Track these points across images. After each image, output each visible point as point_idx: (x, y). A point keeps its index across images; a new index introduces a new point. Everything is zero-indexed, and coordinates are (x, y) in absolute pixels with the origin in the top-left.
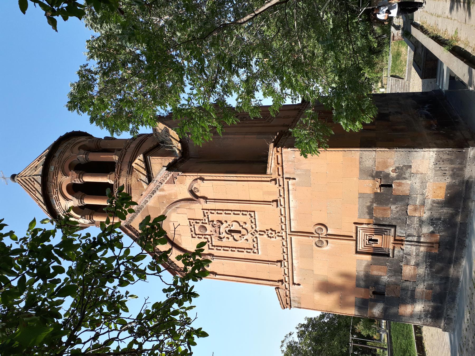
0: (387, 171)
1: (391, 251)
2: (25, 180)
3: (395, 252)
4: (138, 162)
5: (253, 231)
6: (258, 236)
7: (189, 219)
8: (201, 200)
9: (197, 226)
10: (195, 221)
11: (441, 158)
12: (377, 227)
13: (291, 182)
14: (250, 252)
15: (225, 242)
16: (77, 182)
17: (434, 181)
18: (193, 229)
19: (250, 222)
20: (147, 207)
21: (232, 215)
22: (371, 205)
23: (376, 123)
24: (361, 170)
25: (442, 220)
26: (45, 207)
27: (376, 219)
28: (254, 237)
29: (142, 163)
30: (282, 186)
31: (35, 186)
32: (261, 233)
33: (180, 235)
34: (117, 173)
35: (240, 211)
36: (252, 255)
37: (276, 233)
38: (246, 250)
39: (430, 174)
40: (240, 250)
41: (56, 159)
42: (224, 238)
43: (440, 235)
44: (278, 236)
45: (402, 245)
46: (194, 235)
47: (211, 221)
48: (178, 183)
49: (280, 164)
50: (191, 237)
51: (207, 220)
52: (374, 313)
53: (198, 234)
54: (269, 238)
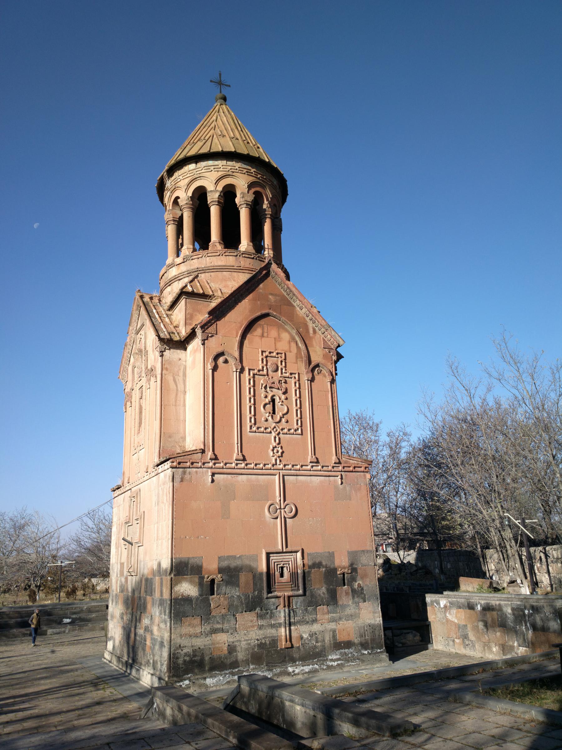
3: (273, 600)
6: (273, 434)
11: (375, 629)
17: (354, 627)
22: (323, 567)
24: (356, 552)
27: (309, 572)
37: (279, 457)
39: (360, 622)
43: (299, 646)
44: (276, 460)
45: (285, 607)
48: (324, 352)
50: (263, 350)
51: (287, 375)
54: (271, 448)
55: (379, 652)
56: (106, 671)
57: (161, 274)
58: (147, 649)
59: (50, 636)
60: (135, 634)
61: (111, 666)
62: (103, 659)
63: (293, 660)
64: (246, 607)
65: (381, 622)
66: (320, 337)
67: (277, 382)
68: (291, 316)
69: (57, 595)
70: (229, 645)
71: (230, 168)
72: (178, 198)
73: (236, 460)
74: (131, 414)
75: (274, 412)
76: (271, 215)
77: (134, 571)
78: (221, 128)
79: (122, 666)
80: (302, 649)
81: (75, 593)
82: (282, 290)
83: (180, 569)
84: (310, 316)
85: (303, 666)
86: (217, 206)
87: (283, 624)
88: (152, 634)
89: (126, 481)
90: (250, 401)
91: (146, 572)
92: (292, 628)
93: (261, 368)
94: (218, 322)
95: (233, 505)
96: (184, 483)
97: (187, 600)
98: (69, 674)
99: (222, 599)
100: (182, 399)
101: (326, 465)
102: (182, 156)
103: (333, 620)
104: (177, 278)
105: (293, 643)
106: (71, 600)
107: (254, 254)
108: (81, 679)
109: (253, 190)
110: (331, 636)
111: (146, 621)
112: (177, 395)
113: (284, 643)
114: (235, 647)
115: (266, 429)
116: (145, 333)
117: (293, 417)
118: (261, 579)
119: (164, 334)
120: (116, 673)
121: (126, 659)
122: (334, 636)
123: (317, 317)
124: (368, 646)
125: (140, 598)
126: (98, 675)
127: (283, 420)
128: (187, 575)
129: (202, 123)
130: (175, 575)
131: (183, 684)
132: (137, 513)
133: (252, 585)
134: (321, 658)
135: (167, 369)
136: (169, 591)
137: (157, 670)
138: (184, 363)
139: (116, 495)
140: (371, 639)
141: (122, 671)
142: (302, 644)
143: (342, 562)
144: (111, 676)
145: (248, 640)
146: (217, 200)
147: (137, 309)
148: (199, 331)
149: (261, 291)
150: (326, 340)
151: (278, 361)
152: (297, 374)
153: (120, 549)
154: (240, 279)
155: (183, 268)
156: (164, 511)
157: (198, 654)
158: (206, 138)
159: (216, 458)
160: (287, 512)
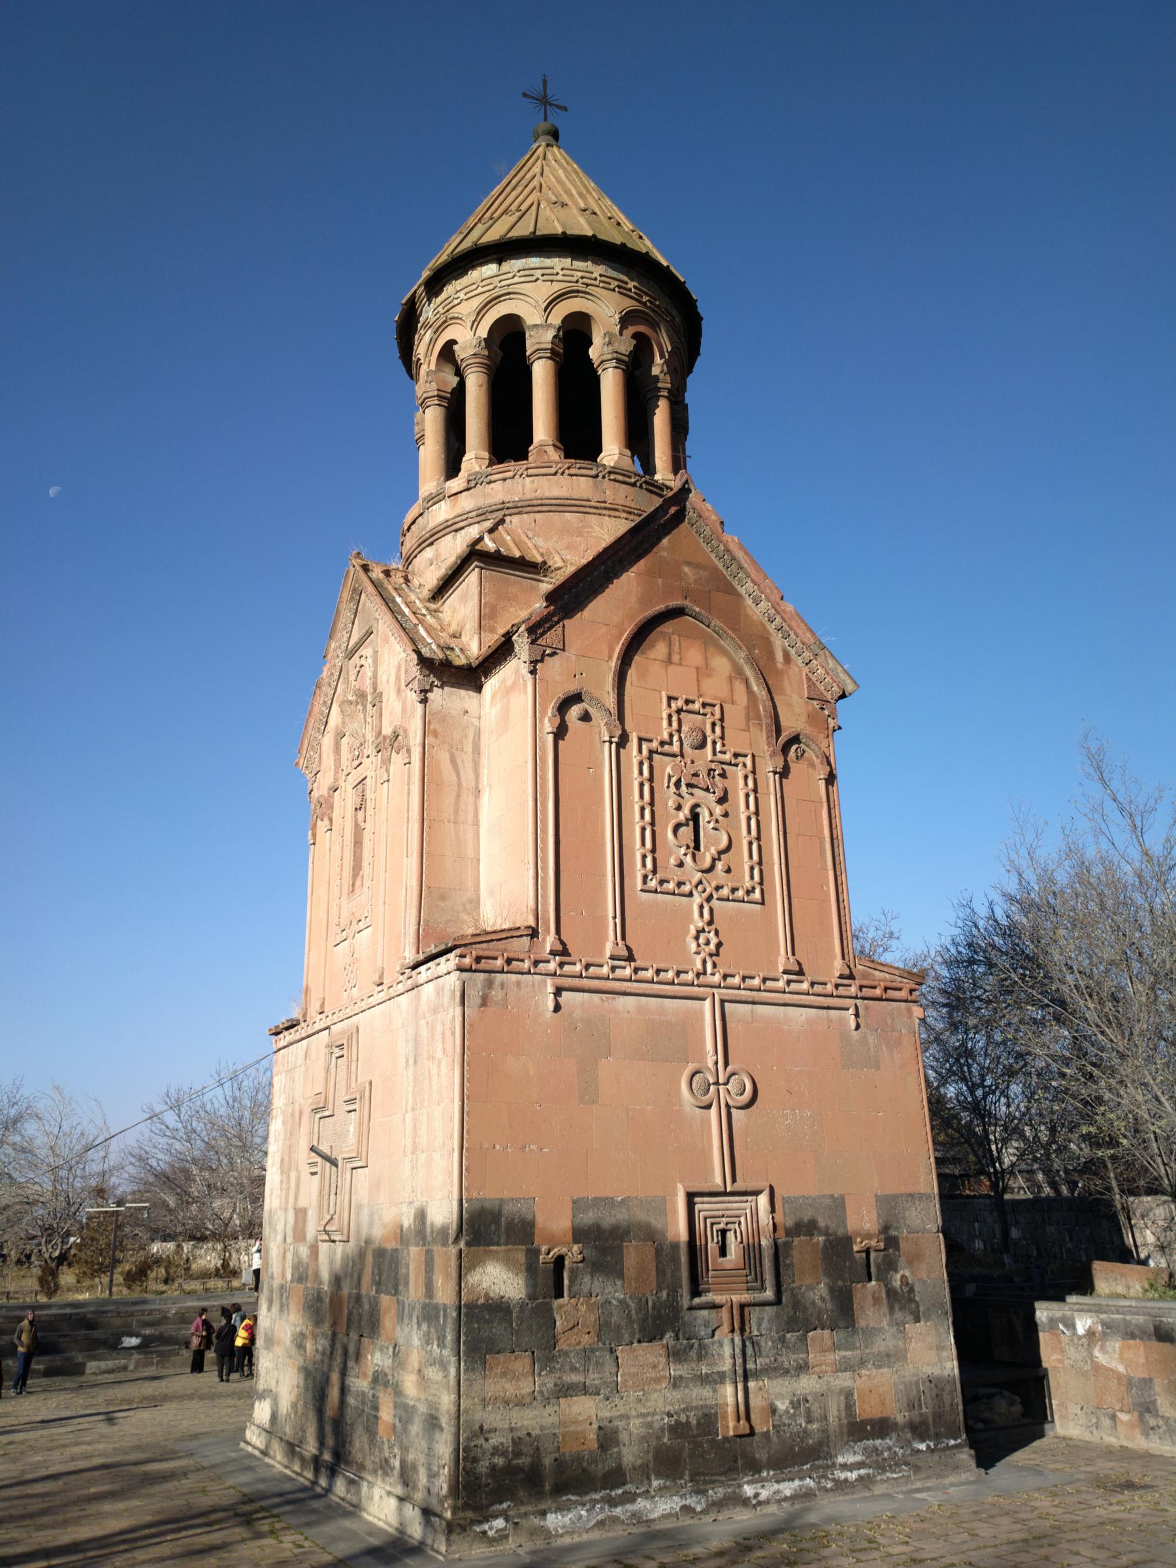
0: (902, 1262)
3: (705, 1313)
6: (697, 899)
11: (943, 1390)
25: (809, 1426)
27: (788, 1245)
33: (669, 661)
36: (633, 869)
37: (711, 955)
43: (768, 1431)
44: (704, 962)
45: (732, 1331)
48: (810, 708)
50: (671, 694)
51: (728, 757)
54: (693, 932)
55: (956, 1446)
56: (263, 1480)
57: (408, 519)
58: (382, 1430)
59: (93, 1378)
60: (343, 1390)
61: (268, 1465)
62: (242, 1445)
63: (754, 1467)
64: (640, 1331)
65: (956, 1371)
66: (800, 671)
67: (703, 773)
68: (734, 618)
69: (106, 1280)
70: (600, 1428)
71: (580, 274)
72: (451, 343)
73: (612, 958)
74: (328, 851)
75: (697, 847)
76: (670, 391)
77: (340, 1230)
78: (557, 189)
79: (303, 1467)
80: (774, 1438)
81: (146, 1275)
82: (713, 556)
83: (482, 1228)
84: (778, 619)
85: (778, 1482)
86: (549, 362)
87: (729, 1374)
88: (398, 1391)
89: (314, 1008)
90: (642, 817)
91: (378, 1233)
92: (752, 1384)
93: (666, 736)
94: (566, 622)
95: (607, 1068)
96: (489, 1010)
97: (498, 1308)
98: (169, 1486)
99: (583, 1308)
100: (471, 808)
101: (821, 979)
102: (467, 244)
103: (845, 1367)
104: (451, 527)
105: (754, 1423)
106: (136, 1295)
107: (636, 475)
108: (205, 1502)
109: (631, 330)
110: (842, 1406)
111: (377, 1359)
112: (458, 796)
113: (731, 1424)
114: (616, 1431)
115: (679, 884)
116: (376, 652)
117: (743, 859)
118: (675, 1260)
119: (432, 650)
120: (288, 1486)
121: (315, 1451)
122: (849, 1407)
123: (793, 624)
124: (928, 1430)
125: (358, 1298)
126: (246, 1490)
127: (720, 866)
128: (498, 1244)
129: (505, 181)
130: (468, 1244)
131: (491, 1528)
132: (348, 1087)
133: (654, 1273)
134: (821, 1462)
135: (435, 734)
136: (453, 1284)
137: (415, 1488)
138: (476, 722)
139: (282, 1044)
140: (934, 1414)
141: (301, 1479)
142: (774, 1426)
144: (280, 1495)
146: (549, 346)
147: (352, 598)
148: (521, 642)
149: (665, 554)
150: (814, 679)
151: (704, 723)
152: (749, 757)
153: (293, 1175)
154: (607, 531)
155: (467, 503)
156: (435, 1079)
157: (525, 1450)
158: (523, 208)
159: (565, 952)
160: (733, 1093)
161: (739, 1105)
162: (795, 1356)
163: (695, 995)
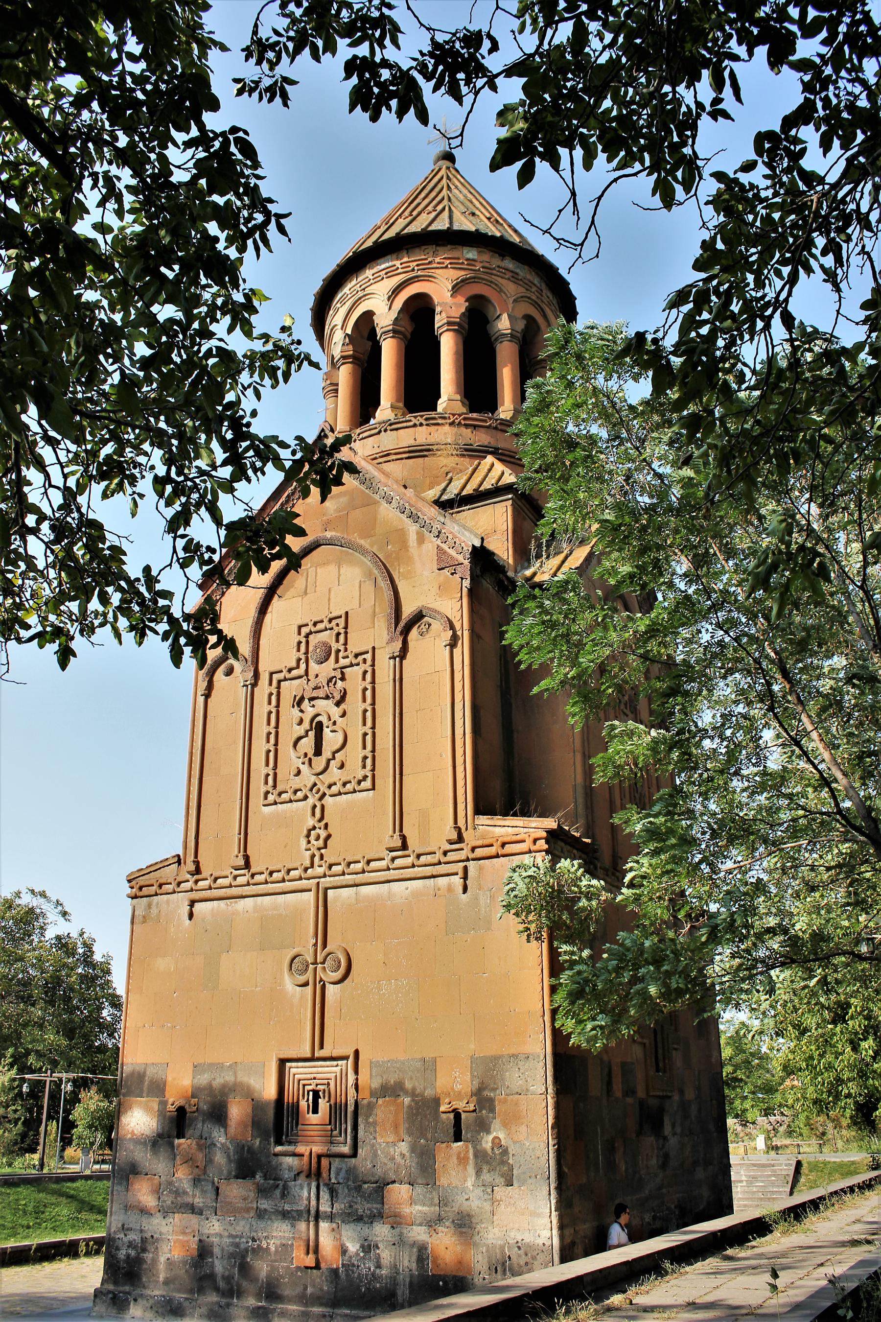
1: (290, 1148)
2: (439, 187)
3: (289, 1160)
4: (497, 472)
5: (323, 789)
6: (311, 801)
7: (347, 613)
8: (399, 644)
9: (330, 636)
10: (342, 631)
12: (351, 1109)
13: (457, 881)
14: (266, 783)
15: (290, 714)
16: (437, 318)
18: (320, 626)
19: (344, 779)
20: (376, 503)
21: (361, 730)
23: (629, 1100)
24: (496, 1059)
25: (378, 1271)
26: (369, 243)
27: (371, 1107)
28: (305, 791)
29: (494, 481)
30: (443, 859)
31: (424, 215)
32: (318, 811)
33: (306, 593)
34: (465, 419)
35: (373, 751)
36: (259, 788)
37: (319, 849)
38: (271, 773)
40: (272, 755)
41: (496, 262)
42: (302, 711)
43: (338, 1269)
44: (313, 856)
46: (305, 630)
47: (342, 673)
48: (442, 578)
49: (502, 850)
50: (301, 623)
51: (346, 662)
52: (129, 1113)
53: (307, 642)
54: (305, 832)
80: (343, 1276)
93: (294, 664)
110: (414, 1258)
142: (343, 1265)
143: (454, 1085)
145: (237, 1236)
161: (332, 980)
162: (369, 1205)
163: (300, 888)
